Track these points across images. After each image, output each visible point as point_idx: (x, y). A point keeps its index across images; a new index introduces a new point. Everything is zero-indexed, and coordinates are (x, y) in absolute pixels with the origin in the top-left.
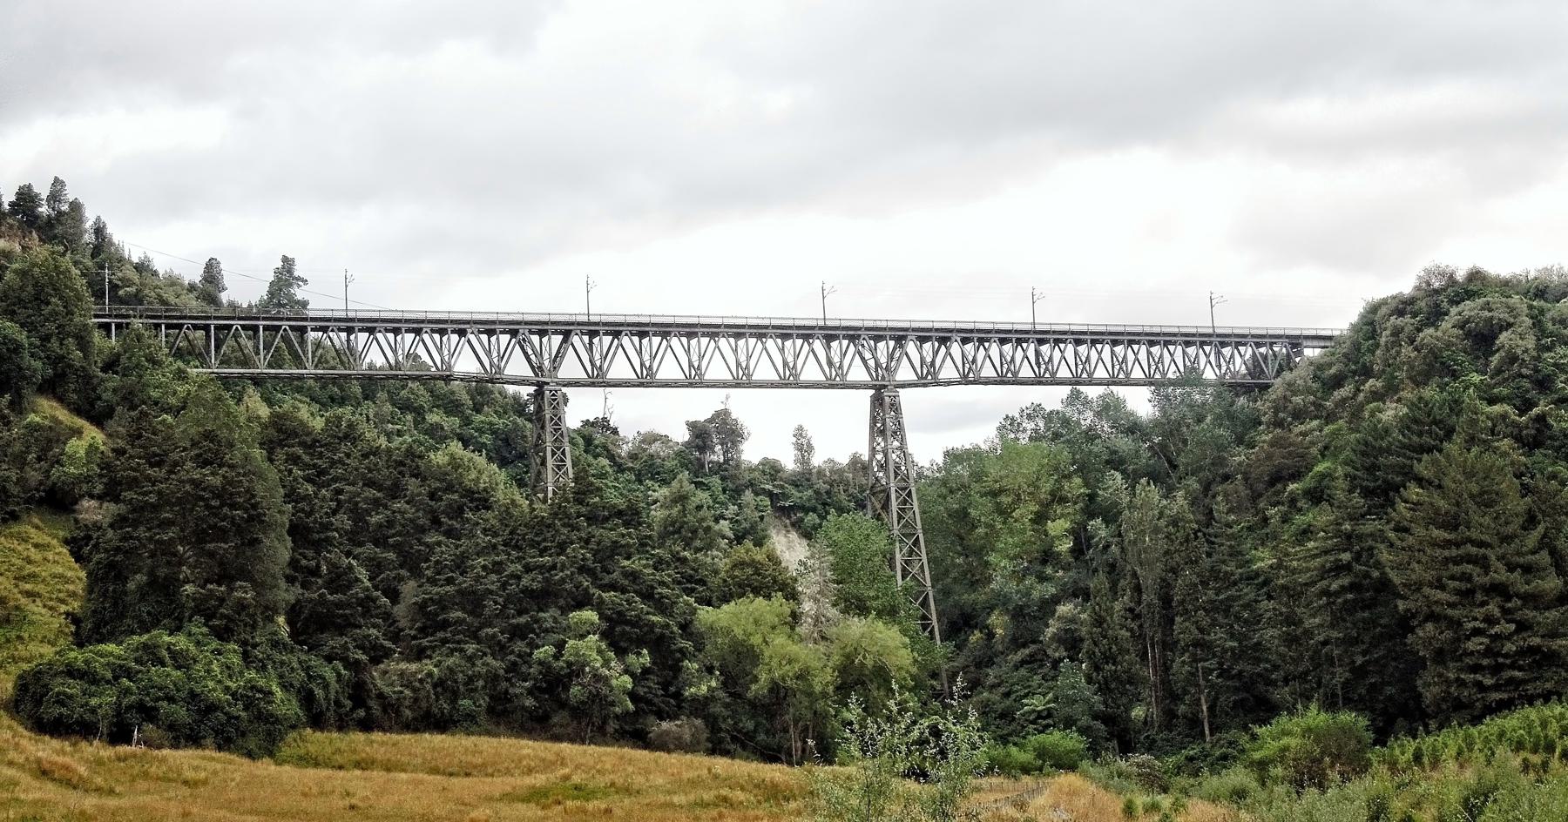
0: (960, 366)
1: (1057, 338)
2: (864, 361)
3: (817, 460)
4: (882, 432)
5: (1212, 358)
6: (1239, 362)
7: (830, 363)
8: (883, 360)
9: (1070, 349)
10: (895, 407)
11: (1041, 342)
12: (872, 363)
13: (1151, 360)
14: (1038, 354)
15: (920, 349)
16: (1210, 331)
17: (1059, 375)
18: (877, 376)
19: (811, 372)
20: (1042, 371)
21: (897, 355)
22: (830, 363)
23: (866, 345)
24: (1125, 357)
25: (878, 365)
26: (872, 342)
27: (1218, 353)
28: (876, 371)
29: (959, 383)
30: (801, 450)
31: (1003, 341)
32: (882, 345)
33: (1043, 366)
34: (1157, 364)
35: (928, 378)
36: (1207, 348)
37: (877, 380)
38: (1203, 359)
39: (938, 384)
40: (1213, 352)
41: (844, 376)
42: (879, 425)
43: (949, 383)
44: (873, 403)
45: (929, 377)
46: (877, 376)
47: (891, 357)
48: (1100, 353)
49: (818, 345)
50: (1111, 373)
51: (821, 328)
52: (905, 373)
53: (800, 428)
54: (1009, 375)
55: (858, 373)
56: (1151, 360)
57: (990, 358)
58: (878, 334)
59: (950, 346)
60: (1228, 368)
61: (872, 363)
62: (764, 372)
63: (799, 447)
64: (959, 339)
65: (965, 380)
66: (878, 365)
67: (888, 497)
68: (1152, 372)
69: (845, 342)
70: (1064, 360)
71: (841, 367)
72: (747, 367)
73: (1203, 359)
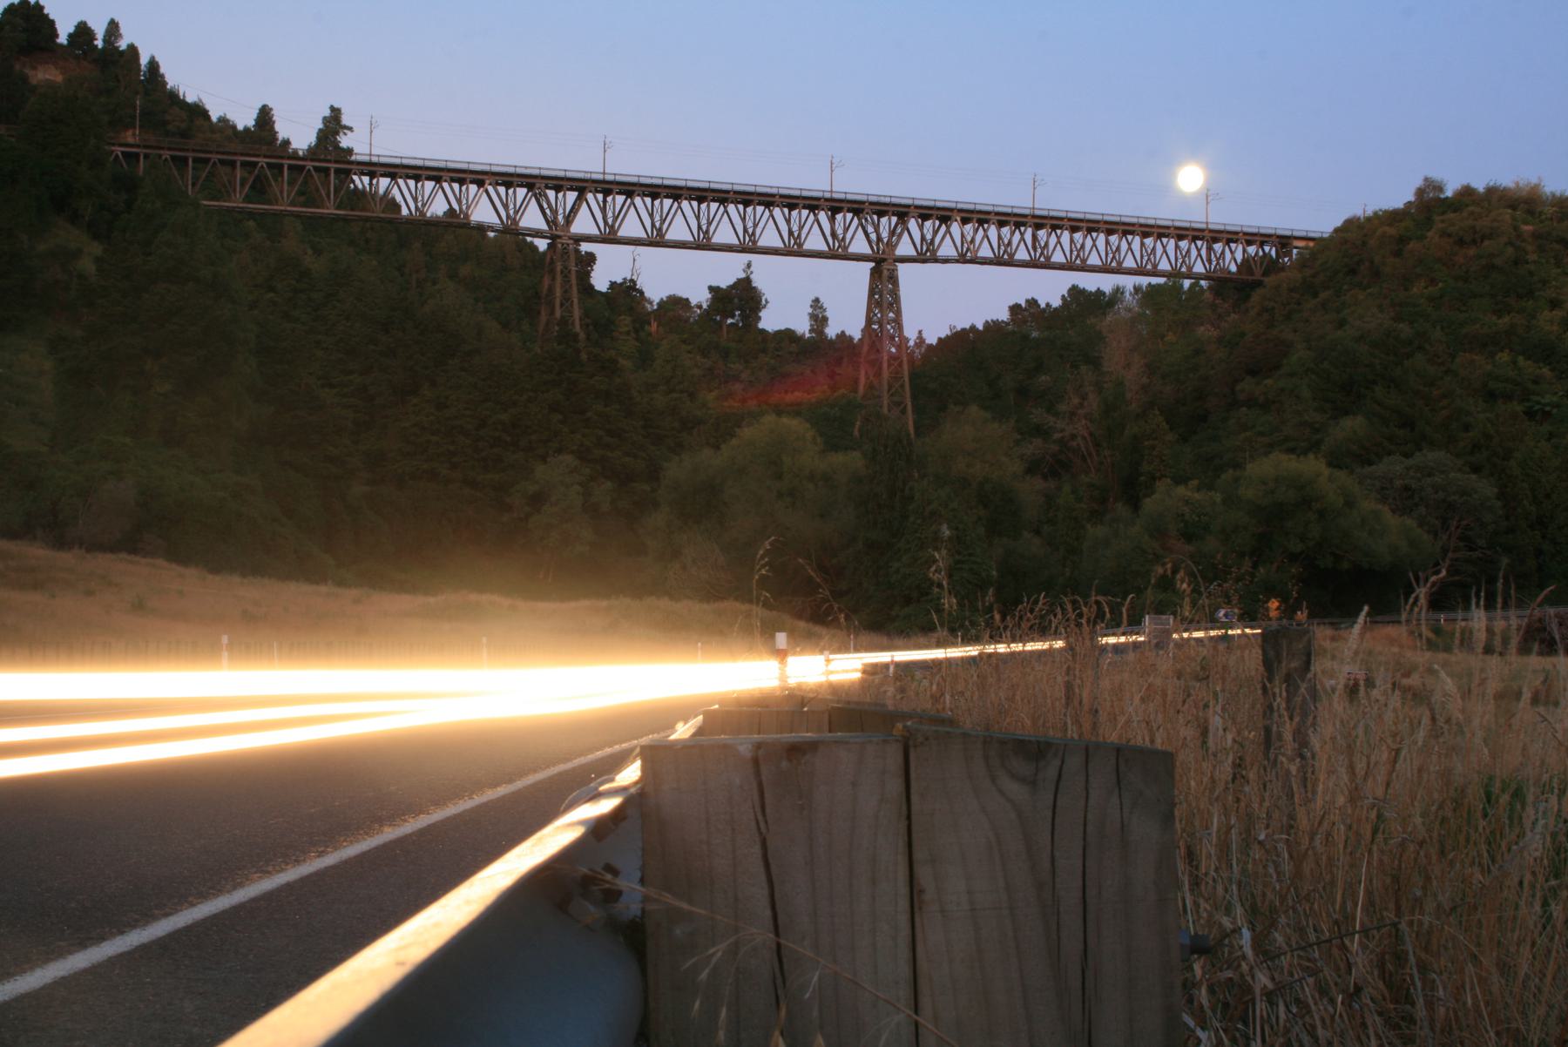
0: (959, 245)
1: (1055, 223)
2: (867, 235)
3: (831, 331)
4: (879, 304)
5: (1204, 252)
6: (1232, 258)
7: (834, 234)
8: (885, 235)
9: (1066, 236)
10: (894, 279)
11: (1038, 227)
12: (873, 236)
13: (1178, 253)
14: (1035, 238)
15: (921, 227)
16: (1204, 226)
17: (1125, 265)
18: (878, 249)
19: (815, 242)
20: (1038, 255)
21: (899, 230)
22: (834, 234)
23: (869, 218)
24: (1154, 249)
25: (879, 239)
26: (875, 217)
27: (1210, 249)
28: (878, 244)
29: (957, 261)
30: (816, 321)
31: (1001, 224)
32: (884, 220)
33: (1039, 250)
34: (1149, 255)
35: (927, 255)
36: (1199, 243)
37: (878, 252)
38: (1194, 253)
39: (936, 260)
40: (1205, 246)
41: (846, 248)
42: (877, 297)
43: (946, 261)
44: (872, 274)
45: (928, 254)
46: (878, 249)
47: (892, 233)
48: (1094, 241)
49: (823, 216)
50: (996, 251)
51: (827, 200)
52: (905, 248)
53: (817, 300)
54: (1006, 257)
55: (860, 245)
56: (1178, 253)
57: (988, 241)
58: (882, 209)
59: (951, 225)
60: (1218, 263)
61: (873, 236)
62: (769, 238)
63: (813, 317)
64: (959, 219)
65: (962, 259)
66: (879, 239)
67: (880, 368)
68: (1144, 262)
69: (849, 216)
70: (1060, 245)
71: (844, 239)
72: (753, 234)
73: (1194, 253)
